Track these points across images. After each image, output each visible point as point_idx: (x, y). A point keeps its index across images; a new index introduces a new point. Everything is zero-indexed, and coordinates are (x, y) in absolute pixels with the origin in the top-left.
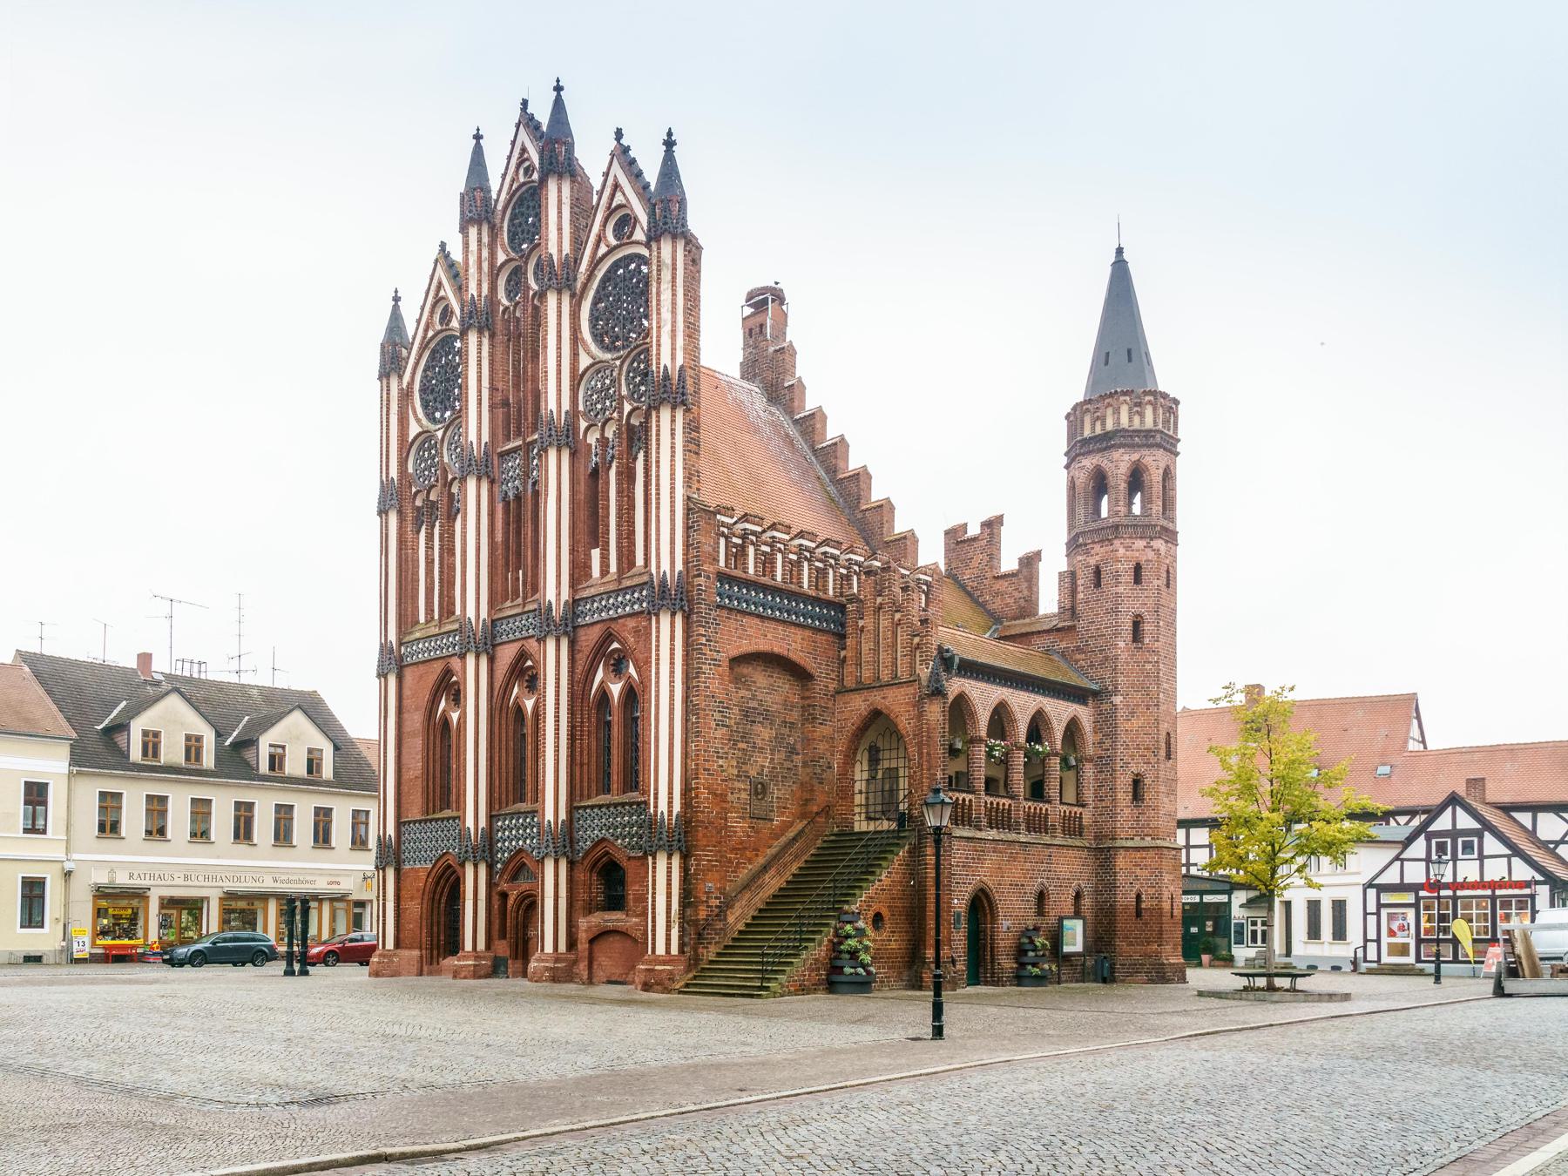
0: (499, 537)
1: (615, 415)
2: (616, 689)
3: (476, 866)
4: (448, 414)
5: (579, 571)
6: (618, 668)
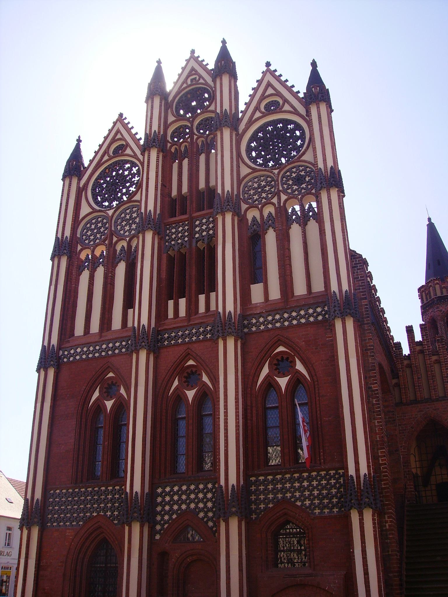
0: (164, 276)
1: (275, 200)
2: (283, 382)
3: (361, 514)
4: (115, 203)
5: (245, 296)
6: (281, 365)
